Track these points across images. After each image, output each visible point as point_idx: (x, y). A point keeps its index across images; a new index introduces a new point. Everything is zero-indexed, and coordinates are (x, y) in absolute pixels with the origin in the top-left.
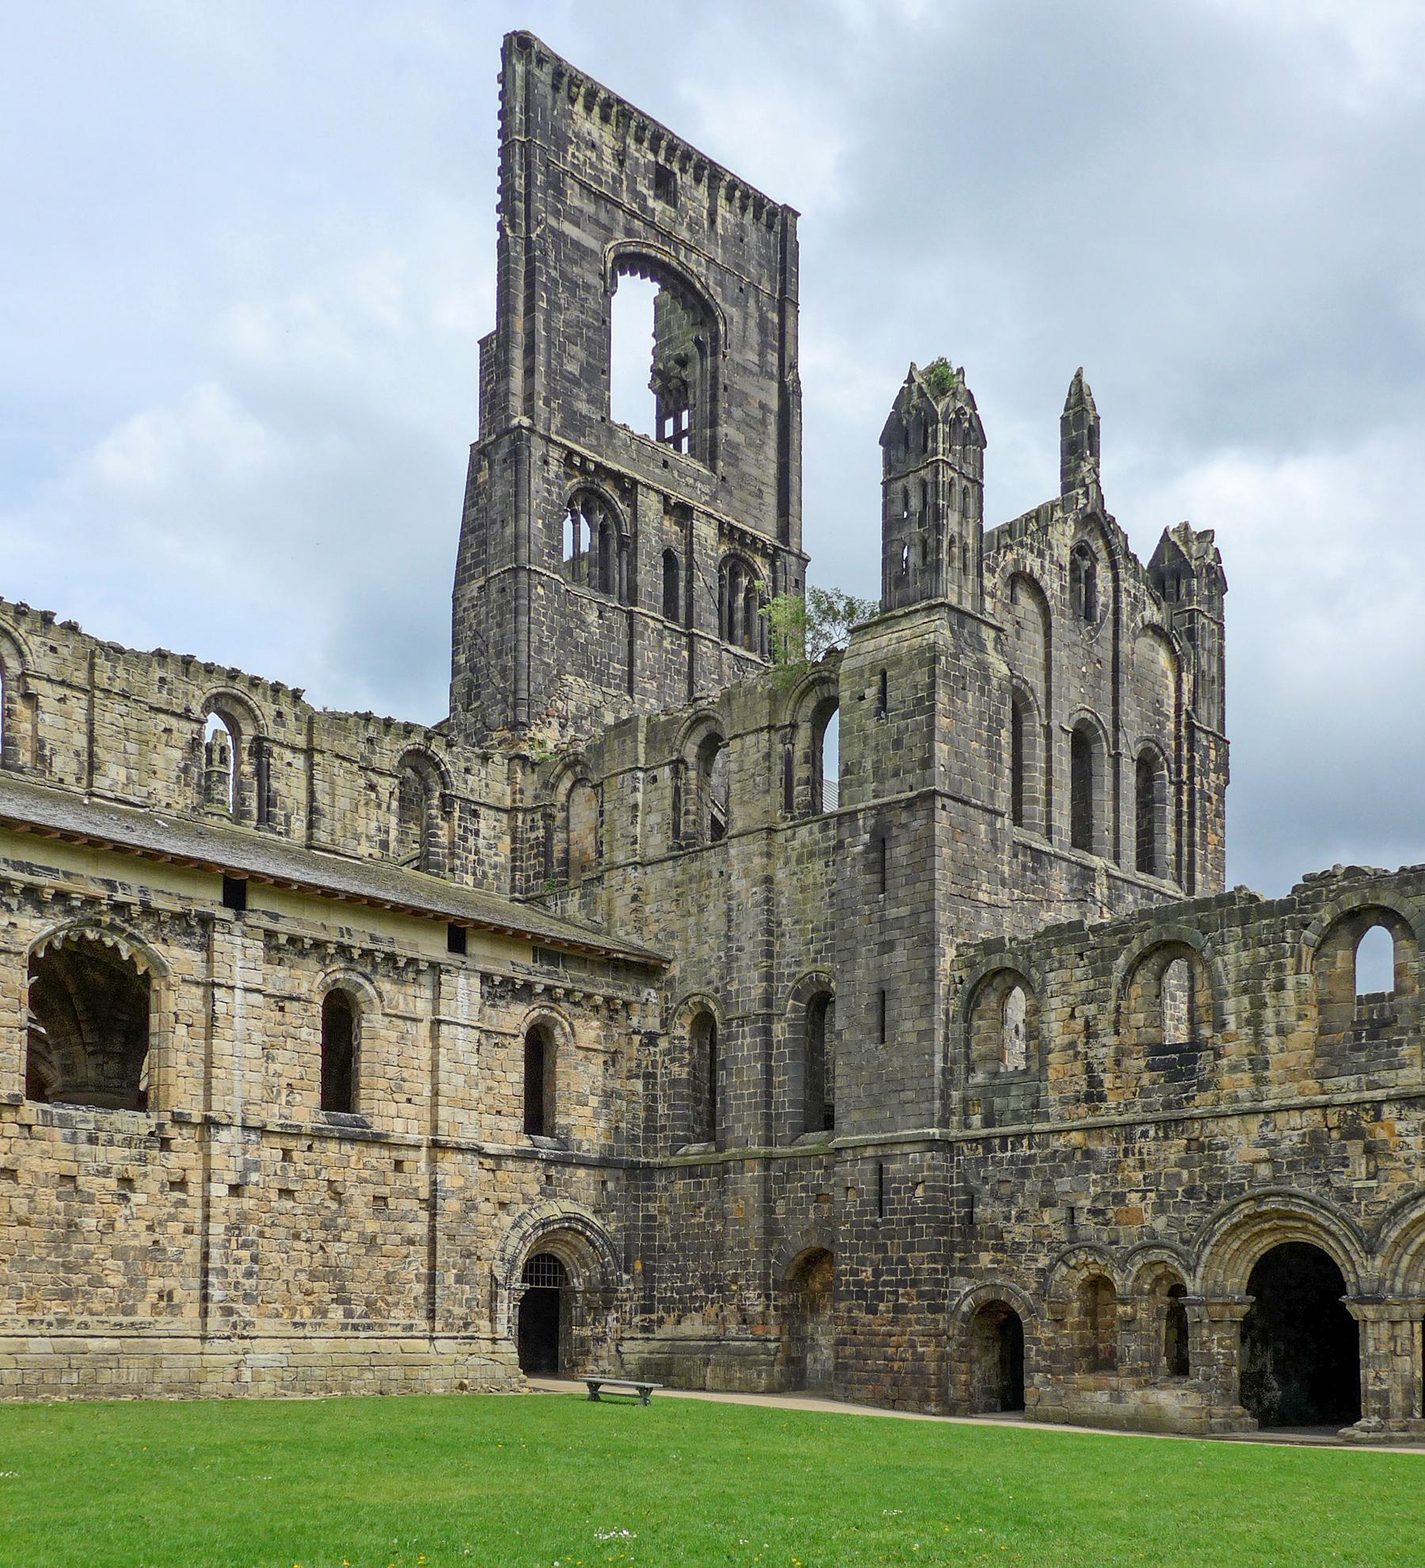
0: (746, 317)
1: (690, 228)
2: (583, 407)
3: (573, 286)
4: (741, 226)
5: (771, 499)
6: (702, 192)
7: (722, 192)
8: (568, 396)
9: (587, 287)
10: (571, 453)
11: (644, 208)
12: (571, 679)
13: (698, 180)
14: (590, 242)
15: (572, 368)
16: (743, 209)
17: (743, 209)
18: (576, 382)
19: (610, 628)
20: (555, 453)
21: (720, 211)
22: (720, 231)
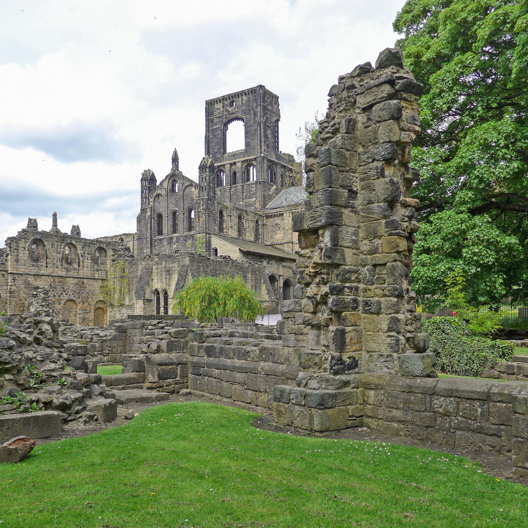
2: (218, 156)
3: (215, 136)
13: (239, 97)
16: (249, 94)
18: (217, 152)
22: (244, 102)
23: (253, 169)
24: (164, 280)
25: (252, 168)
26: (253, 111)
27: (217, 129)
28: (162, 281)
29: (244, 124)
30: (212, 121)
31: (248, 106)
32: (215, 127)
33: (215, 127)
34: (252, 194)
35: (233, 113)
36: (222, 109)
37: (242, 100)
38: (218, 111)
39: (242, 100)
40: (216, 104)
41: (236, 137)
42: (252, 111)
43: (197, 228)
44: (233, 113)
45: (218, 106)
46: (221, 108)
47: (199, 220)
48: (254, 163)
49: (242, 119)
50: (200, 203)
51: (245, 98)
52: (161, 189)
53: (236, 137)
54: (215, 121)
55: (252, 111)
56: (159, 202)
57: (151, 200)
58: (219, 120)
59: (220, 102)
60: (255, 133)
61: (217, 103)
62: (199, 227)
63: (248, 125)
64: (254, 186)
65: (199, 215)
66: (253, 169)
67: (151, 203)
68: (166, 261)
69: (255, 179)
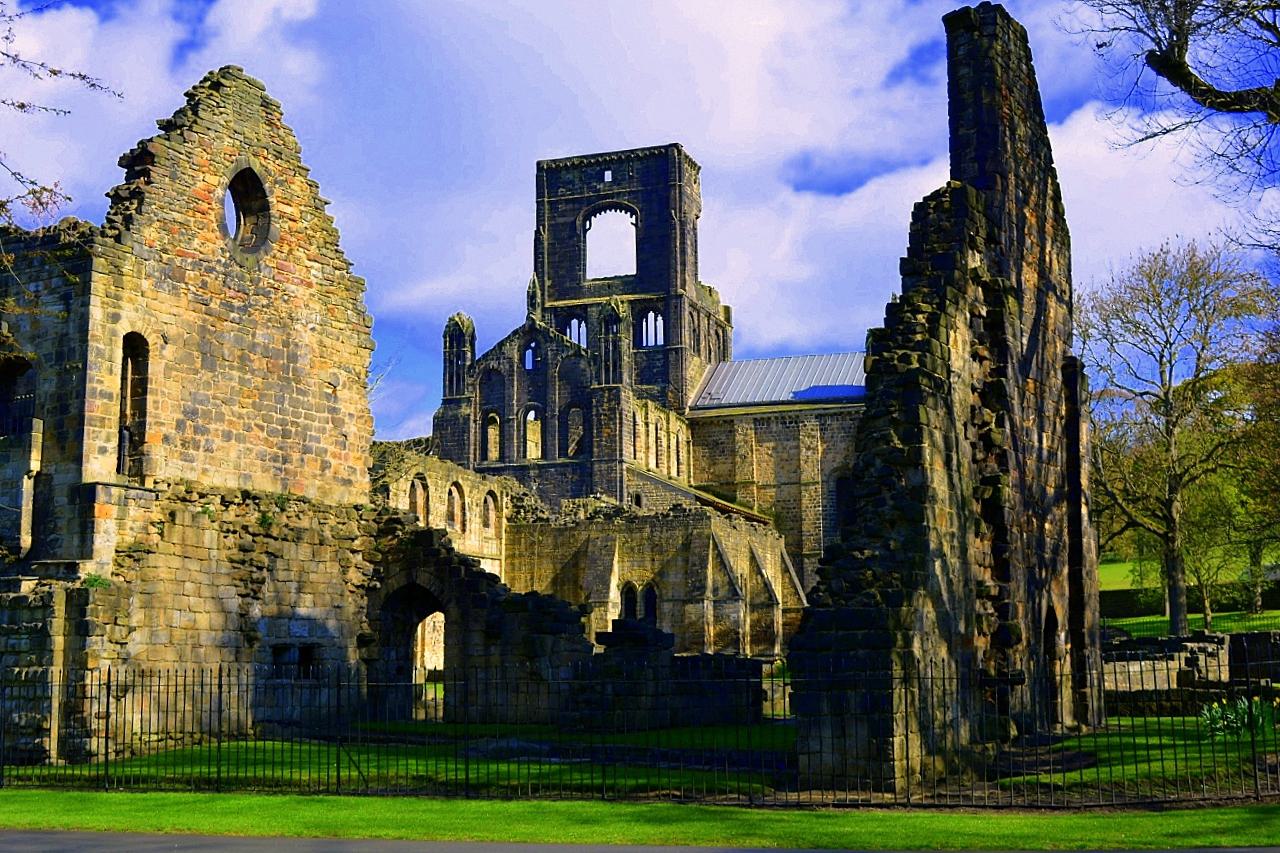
2: (568, 285)
18: (564, 277)
23: (656, 320)
24: (648, 565)
25: (651, 315)
28: (641, 565)
29: (633, 220)
32: (561, 220)
33: (561, 220)
34: (655, 374)
40: (564, 172)
41: (611, 244)
43: (595, 450)
46: (577, 181)
47: (599, 433)
48: (660, 305)
49: (627, 209)
50: (602, 396)
51: (637, 165)
52: (498, 359)
53: (611, 244)
58: (570, 206)
62: (599, 446)
64: (660, 356)
65: (599, 421)
66: (656, 320)
68: (653, 526)
69: (661, 341)
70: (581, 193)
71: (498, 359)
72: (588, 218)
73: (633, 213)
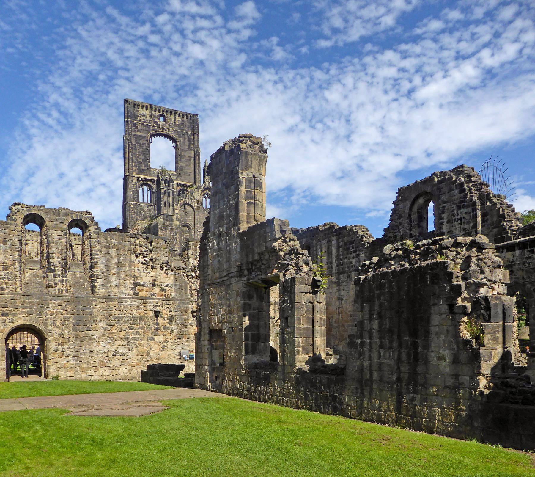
0: (184, 140)
1: (169, 125)
2: (143, 168)
3: (140, 144)
4: (183, 121)
5: (192, 175)
6: (172, 117)
7: (177, 115)
8: (139, 166)
9: (143, 144)
10: (139, 178)
11: (157, 124)
12: (140, 221)
13: (171, 115)
14: (144, 135)
15: (140, 160)
16: (183, 118)
17: (183, 118)
18: (141, 163)
19: (150, 210)
20: (135, 179)
21: (177, 119)
22: (177, 123)
26: (188, 137)
27: (141, 136)
30: (135, 126)
31: (182, 130)
35: (163, 129)
36: (148, 118)
37: (175, 120)
38: (144, 118)
39: (175, 120)
40: (140, 109)
42: (186, 136)
44: (163, 129)
45: (145, 114)
46: (148, 116)
51: (178, 118)
54: (139, 127)
55: (186, 136)
56: (186, 214)
57: (175, 207)
58: (144, 128)
59: (147, 109)
60: (190, 160)
61: (143, 109)
63: (182, 148)
67: (176, 212)
70: (150, 123)
71: (191, 199)
72: (151, 137)
73: (174, 141)
